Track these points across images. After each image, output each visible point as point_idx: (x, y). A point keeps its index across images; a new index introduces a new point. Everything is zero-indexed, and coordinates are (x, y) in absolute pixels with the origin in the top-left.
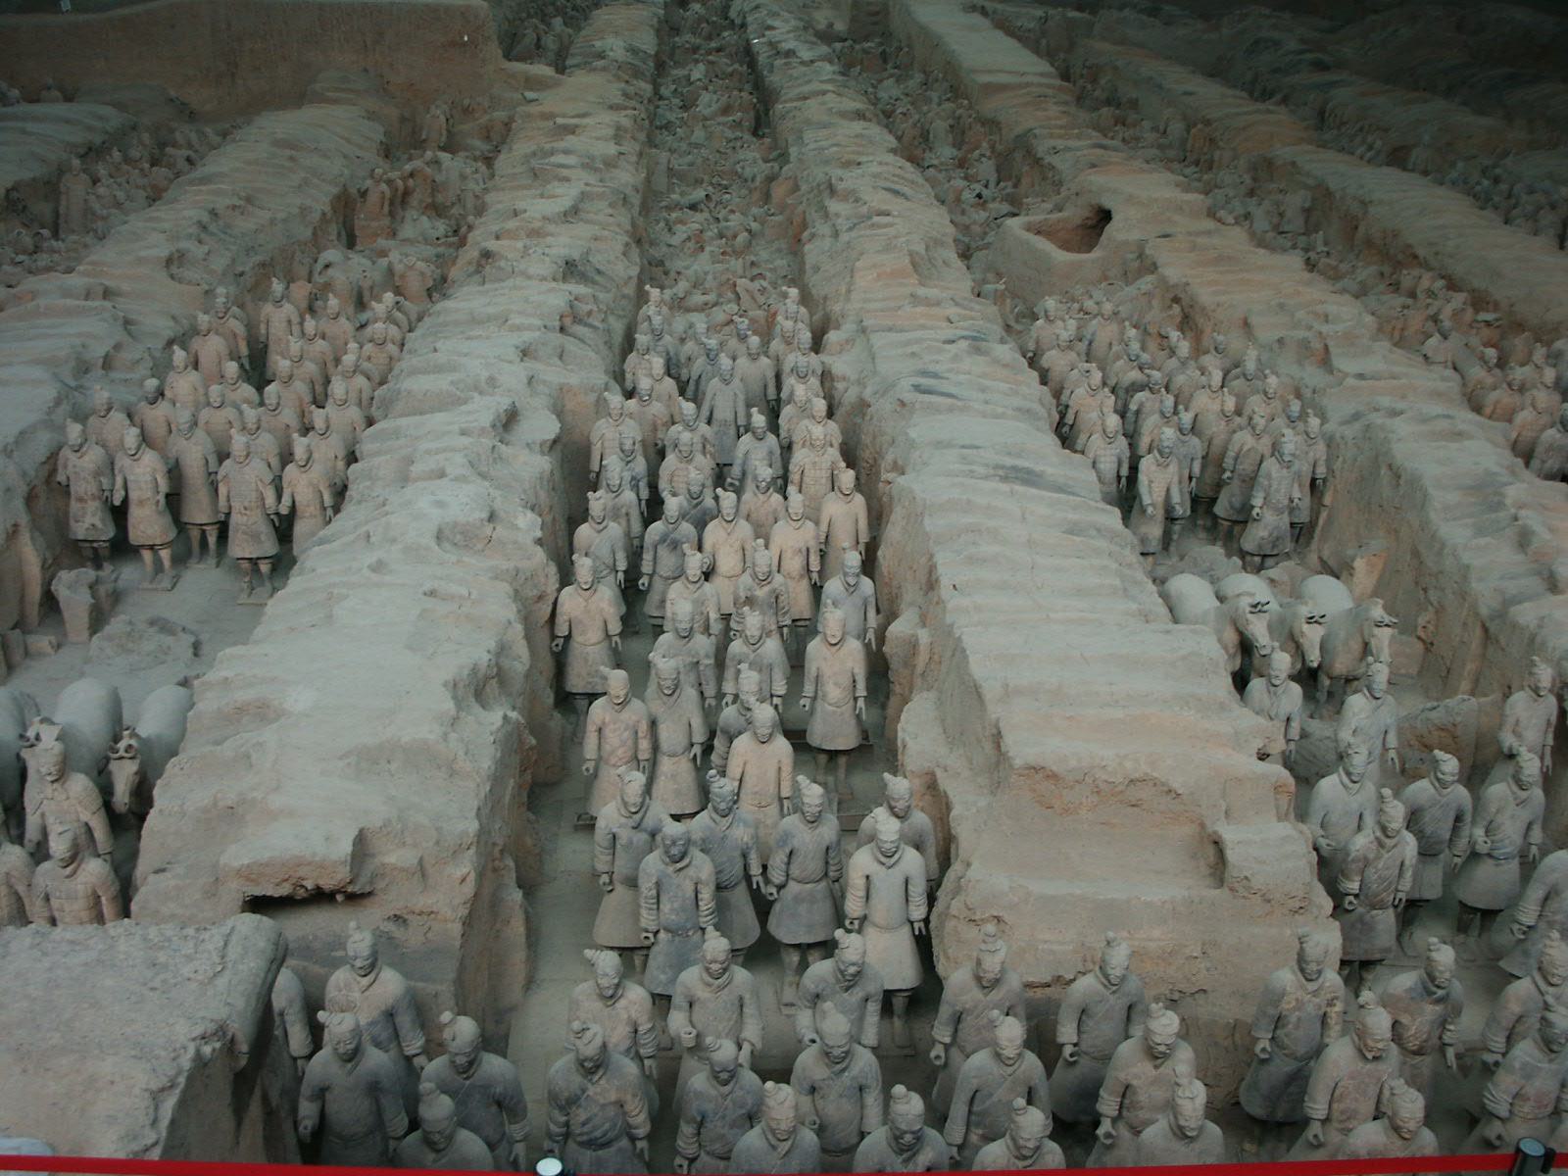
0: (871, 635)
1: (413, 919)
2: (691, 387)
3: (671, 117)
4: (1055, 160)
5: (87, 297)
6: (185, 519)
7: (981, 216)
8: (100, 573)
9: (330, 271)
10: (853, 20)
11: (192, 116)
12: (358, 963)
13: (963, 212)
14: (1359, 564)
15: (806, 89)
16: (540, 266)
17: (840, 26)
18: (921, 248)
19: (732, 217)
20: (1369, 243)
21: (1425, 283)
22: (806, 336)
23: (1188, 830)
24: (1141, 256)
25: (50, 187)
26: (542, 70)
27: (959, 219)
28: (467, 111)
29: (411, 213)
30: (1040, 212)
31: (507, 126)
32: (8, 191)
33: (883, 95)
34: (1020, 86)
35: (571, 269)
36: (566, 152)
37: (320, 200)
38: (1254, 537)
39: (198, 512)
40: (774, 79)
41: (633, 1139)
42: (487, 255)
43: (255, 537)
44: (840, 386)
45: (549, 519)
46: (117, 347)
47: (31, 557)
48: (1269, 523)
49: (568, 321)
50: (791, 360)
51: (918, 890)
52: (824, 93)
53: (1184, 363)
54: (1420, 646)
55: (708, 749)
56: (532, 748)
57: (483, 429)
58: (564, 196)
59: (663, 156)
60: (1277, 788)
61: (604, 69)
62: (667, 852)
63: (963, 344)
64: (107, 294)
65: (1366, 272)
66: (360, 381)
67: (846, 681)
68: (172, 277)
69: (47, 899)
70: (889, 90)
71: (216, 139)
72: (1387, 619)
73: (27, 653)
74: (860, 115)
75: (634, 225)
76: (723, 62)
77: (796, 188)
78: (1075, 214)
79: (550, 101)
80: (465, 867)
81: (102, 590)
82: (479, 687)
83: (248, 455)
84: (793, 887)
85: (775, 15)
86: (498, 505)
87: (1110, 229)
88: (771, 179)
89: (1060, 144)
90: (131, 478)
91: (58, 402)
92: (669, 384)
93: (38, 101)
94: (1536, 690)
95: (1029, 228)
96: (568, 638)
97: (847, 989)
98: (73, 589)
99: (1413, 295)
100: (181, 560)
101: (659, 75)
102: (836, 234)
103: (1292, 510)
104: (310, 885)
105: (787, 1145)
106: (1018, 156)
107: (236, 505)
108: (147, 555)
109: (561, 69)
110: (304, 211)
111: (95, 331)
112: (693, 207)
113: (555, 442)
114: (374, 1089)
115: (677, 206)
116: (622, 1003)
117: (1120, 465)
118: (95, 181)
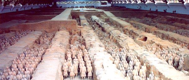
4: (137, 33)
11: (47, 32)
15: (108, 27)
20: (170, 38)
21: (179, 42)
24: (152, 41)
25: (39, 40)
29: (75, 41)
31: (80, 33)
38: (180, 67)
40: (103, 26)
43: (84, 75)
48: (181, 66)
71: (53, 35)
77: (113, 37)
95: (138, 39)
102: (122, 41)
108: (71, 77)
112: (102, 39)
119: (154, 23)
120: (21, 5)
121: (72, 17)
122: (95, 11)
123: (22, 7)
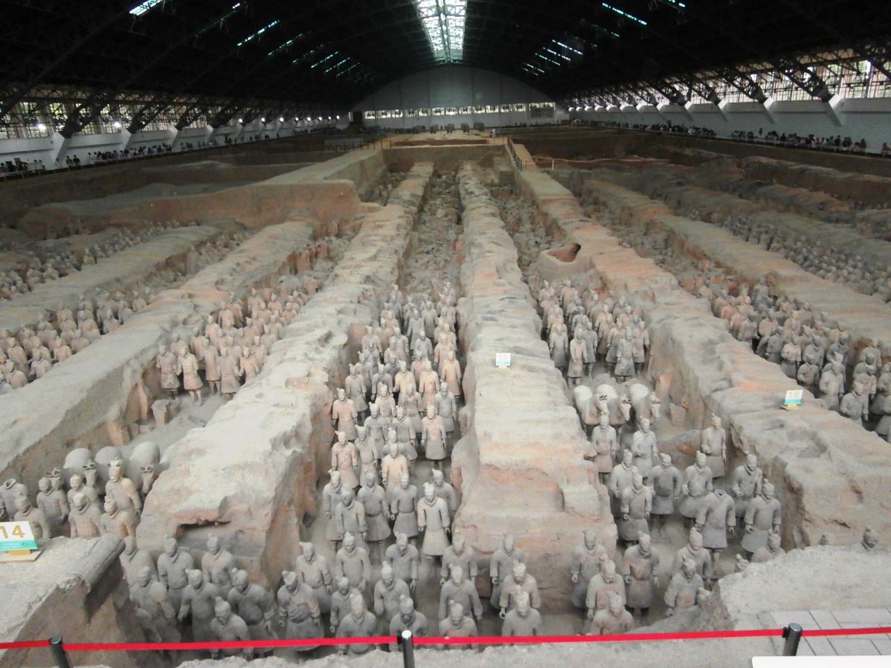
0: (454, 415)
1: (246, 531)
2: (406, 322)
3: (426, 219)
5: (182, 297)
6: (207, 379)
7: (536, 249)
8: (173, 401)
9: (283, 285)
10: (501, 179)
12: (212, 550)
13: (529, 249)
14: (662, 378)
16: (356, 278)
17: (496, 181)
18: (501, 265)
19: (442, 256)
20: (689, 251)
22: (449, 300)
23: (551, 489)
24: (591, 262)
25: (184, 257)
26: (375, 205)
27: (526, 251)
28: (347, 221)
29: (320, 260)
30: (556, 247)
31: (360, 225)
32: (167, 260)
33: (508, 206)
34: (557, 200)
35: (368, 279)
36: (375, 235)
37: (283, 257)
38: (618, 371)
39: (211, 376)
40: (464, 203)
41: (313, 618)
42: (336, 276)
44: (462, 318)
45: (337, 374)
46: (190, 316)
47: (143, 396)
48: (624, 364)
49: (361, 299)
50: (444, 309)
51: (445, 515)
52: (481, 207)
53: (597, 303)
54: (683, 409)
55: (380, 461)
56: (311, 463)
57: (314, 342)
58: (372, 251)
59: (416, 234)
60: (589, 471)
61: (398, 203)
62: (343, 503)
63: (506, 300)
64: (190, 296)
65: (686, 262)
66: (279, 325)
67: (437, 432)
68: (218, 289)
69: (105, 527)
70: (511, 204)
72: (658, 400)
73: (139, 432)
74: (493, 215)
75: (399, 260)
76: (449, 198)
78: (569, 247)
79: (377, 216)
80: (268, 510)
81: (172, 407)
82: (286, 441)
83: (227, 354)
84: (401, 515)
85: (470, 179)
86: (312, 370)
87: (580, 252)
88: (456, 240)
89: (567, 221)
90: (184, 365)
91: (160, 337)
92: (395, 322)
93: (187, 226)
94: (715, 427)
95: (550, 254)
96: (338, 420)
97: (402, 556)
98: (159, 408)
99: (703, 271)
100: (205, 395)
101: (425, 203)
102: (472, 260)
103: (634, 358)
104: (203, 519)
105: (360, 621)
106: (554, 226)
107: (224, 374)
108: (192, 393)
109: (385, 205)
110: (275, 263)
111: (183, 312)
113: (345, 345)
114: (210, 600)
115: (422, 252)
116: (314, 564)
117: (564, 343)
118: (201, 254)
119: (684, 188)
120: (210, 129)
121: (385, 167)
122: (484, 142)
123: (214, 134)
